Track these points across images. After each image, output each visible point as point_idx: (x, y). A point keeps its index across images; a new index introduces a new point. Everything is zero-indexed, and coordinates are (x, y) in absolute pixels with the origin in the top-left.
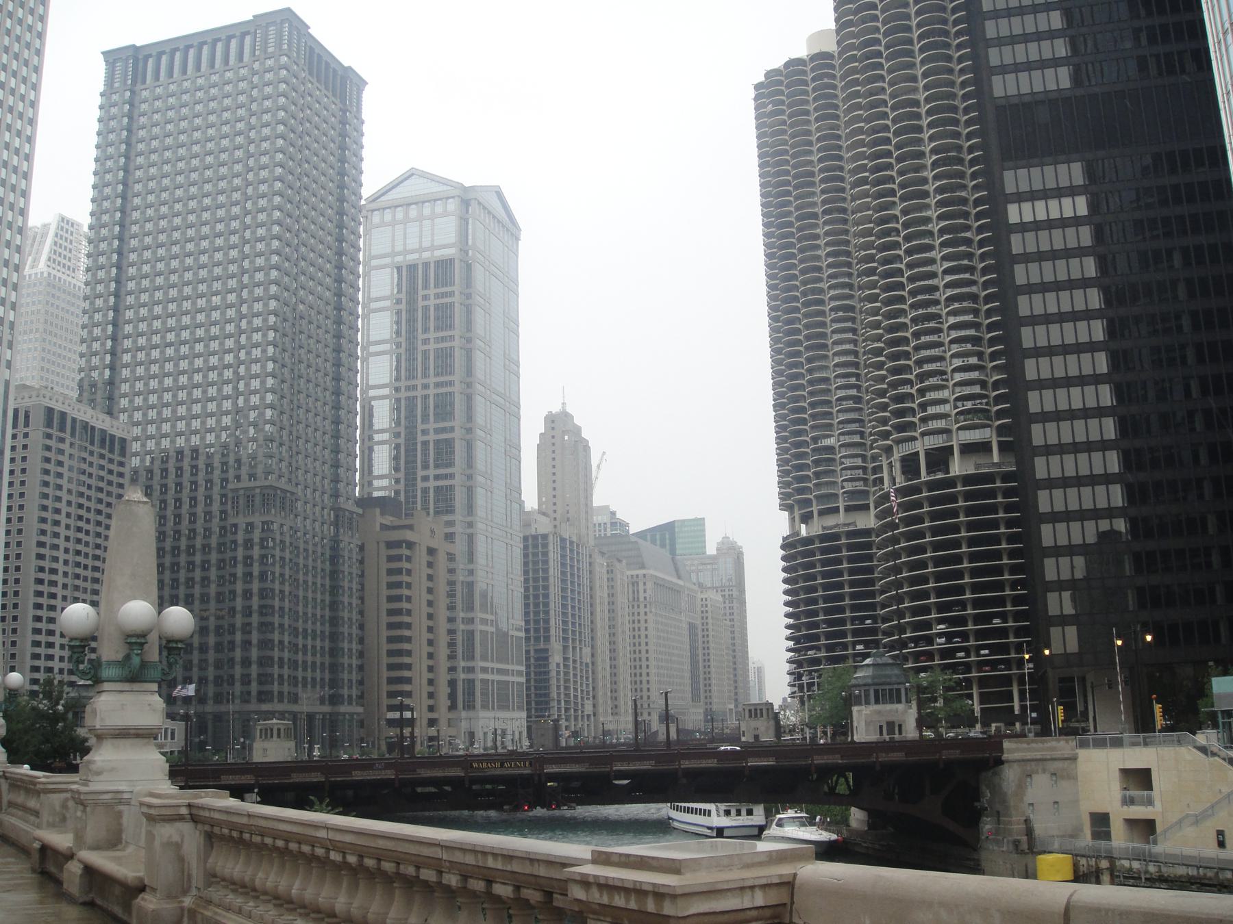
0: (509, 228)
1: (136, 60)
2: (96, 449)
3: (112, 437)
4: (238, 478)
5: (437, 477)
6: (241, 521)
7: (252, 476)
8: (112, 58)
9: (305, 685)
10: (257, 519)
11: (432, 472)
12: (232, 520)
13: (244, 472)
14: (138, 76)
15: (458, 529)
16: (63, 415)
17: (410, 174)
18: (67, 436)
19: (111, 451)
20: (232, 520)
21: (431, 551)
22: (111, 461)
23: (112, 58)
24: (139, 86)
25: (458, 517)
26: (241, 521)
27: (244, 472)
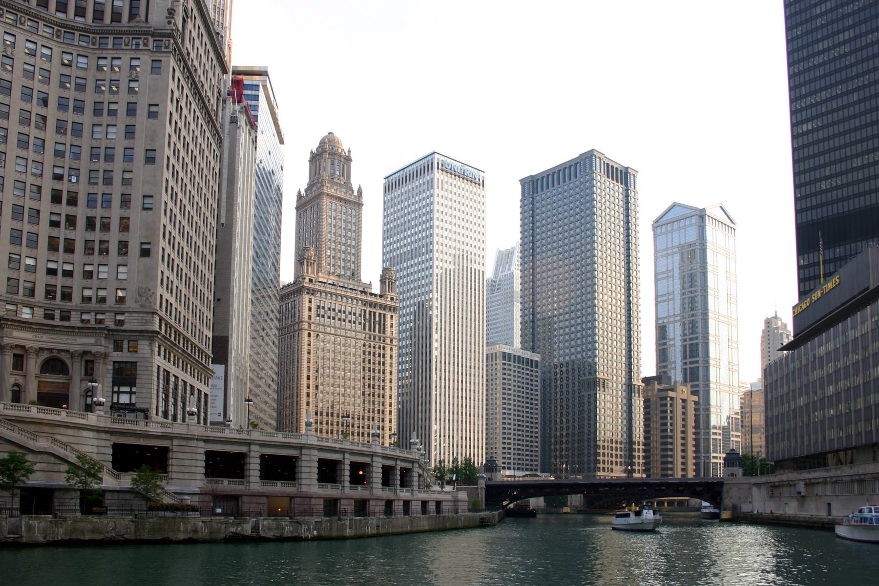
0: (730, 224)
1: (533, 182)
2: (525, 367)
3: (532, 361)
4: (584, 374)
5: (691, 363)
6: (585, 393)
7: (590, 373)
8: (523, 182)
9: (616, 464)
10: (592, 393)
11: (688, 361)
12: (582, 393)
13: (586, 372)
14: (535, 190)
15: (701, 388)
16: (510, 354)
17: (674, 206)
18: (512, 363)
19: (532, 366)
20: (582, 393)
21: (684, 401)
22: (532, 371)
23: (523, 182)
24: (535, 195)
25: (701, 383)
26: (585, 393)
27: (586, 372)
